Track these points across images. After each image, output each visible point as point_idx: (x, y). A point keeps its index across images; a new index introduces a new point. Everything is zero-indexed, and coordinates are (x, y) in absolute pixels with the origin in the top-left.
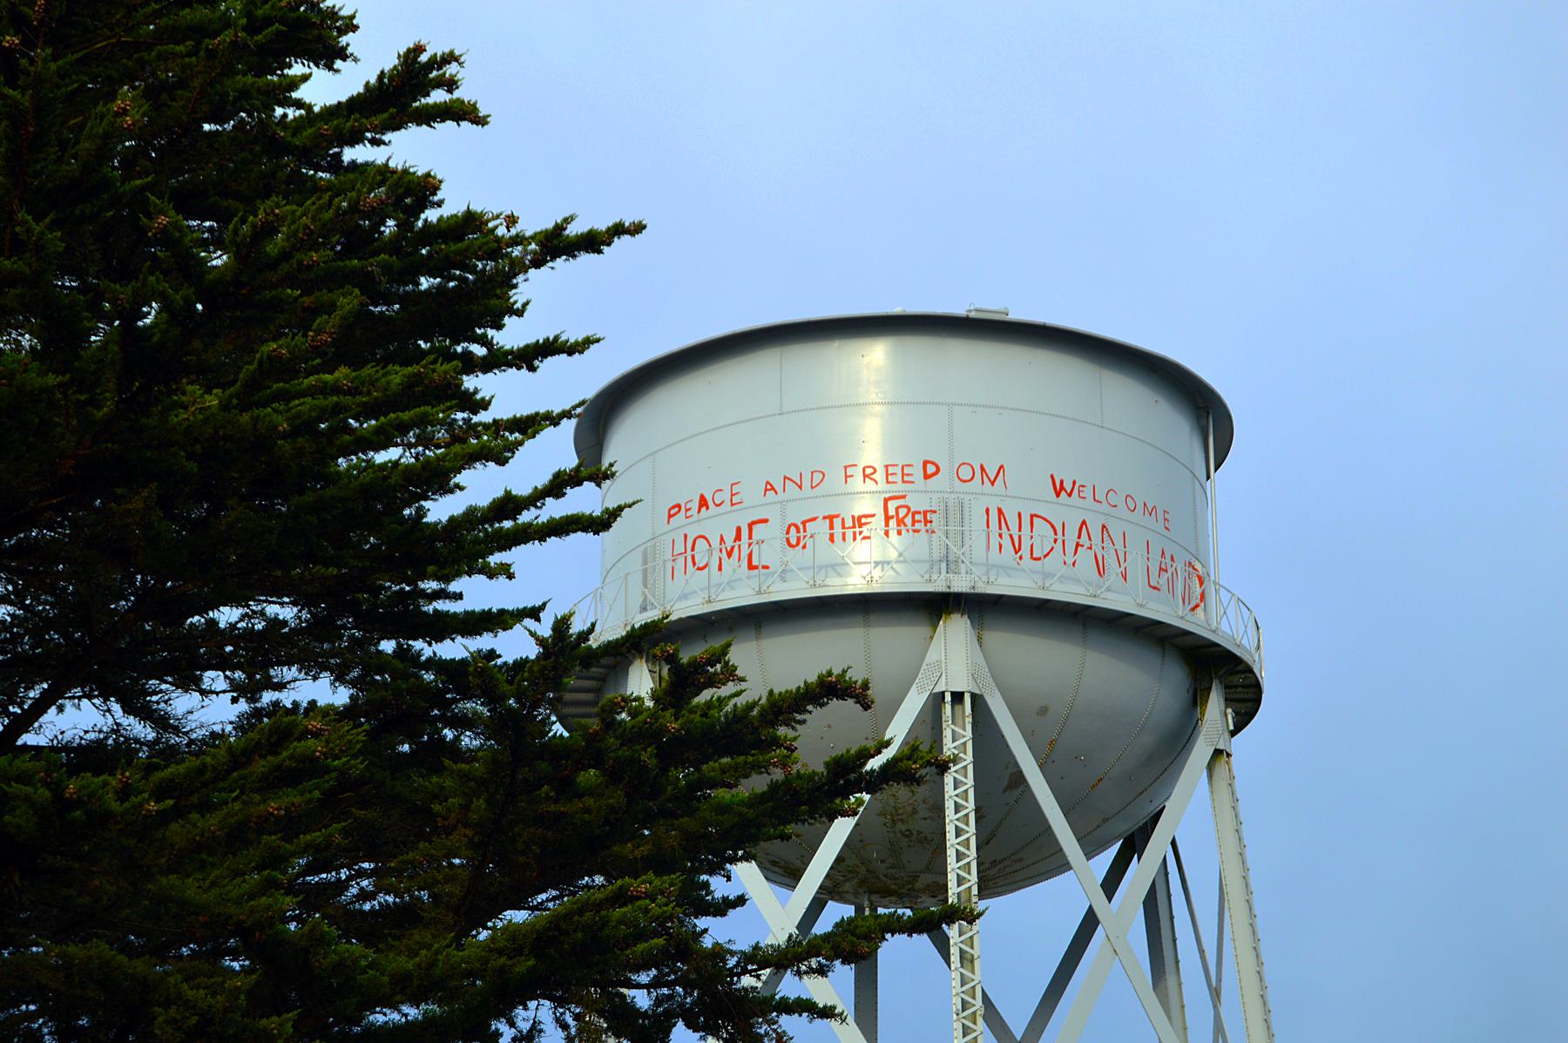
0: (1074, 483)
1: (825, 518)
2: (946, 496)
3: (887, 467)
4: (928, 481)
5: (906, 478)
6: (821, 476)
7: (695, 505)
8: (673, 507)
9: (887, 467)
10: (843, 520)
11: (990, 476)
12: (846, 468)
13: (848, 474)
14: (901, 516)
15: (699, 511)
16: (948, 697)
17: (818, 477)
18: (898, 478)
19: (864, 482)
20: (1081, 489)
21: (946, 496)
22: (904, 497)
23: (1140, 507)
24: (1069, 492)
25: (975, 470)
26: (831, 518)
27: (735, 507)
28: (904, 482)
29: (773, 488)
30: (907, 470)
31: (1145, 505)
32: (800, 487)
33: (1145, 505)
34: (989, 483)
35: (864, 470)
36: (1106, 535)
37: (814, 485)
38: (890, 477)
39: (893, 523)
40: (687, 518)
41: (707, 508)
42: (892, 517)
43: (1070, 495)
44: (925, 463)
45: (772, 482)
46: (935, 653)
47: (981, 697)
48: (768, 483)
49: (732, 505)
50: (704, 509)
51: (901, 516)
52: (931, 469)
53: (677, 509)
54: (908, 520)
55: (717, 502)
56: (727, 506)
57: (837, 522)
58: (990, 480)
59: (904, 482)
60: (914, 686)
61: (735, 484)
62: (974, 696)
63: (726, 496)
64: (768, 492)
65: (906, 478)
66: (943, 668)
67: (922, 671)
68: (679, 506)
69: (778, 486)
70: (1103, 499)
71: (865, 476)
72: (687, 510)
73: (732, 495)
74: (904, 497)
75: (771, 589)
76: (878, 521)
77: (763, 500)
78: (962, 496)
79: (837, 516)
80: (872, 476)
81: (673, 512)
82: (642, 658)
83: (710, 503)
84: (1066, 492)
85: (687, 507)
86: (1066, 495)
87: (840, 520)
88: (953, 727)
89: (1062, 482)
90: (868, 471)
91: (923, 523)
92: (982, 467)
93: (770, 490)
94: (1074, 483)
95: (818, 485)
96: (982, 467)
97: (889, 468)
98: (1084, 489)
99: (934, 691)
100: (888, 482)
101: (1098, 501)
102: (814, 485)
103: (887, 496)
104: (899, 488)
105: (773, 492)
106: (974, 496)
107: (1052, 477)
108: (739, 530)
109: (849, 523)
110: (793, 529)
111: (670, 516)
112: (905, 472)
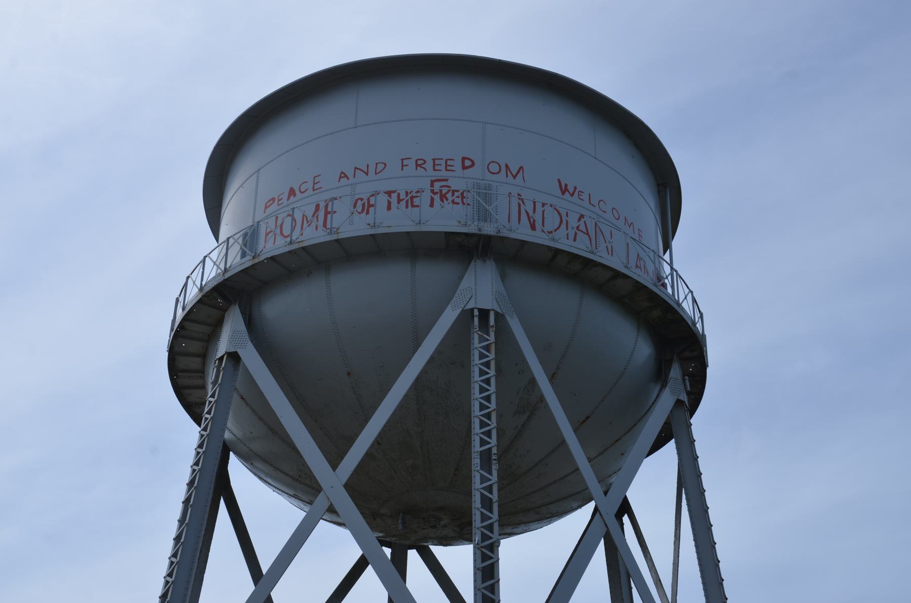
0: (575, 188)
1: (386, 193)
2: (479, 181)
3: (434, 160)
5: (448, 168)
6: (383, 165)
7: (286, 195)
8: (269, 201)
9: (434, 160)
10: (399, 194)
11: (513, 173)
12: (402, 160)
13: (404, 164)
14: (444, 191)
16: (476, 313)
17: (381, 167)
18: (443, 167)
19: (416, 169)
20: (580, 193)
21: (479, 181)
22: (447, 180)
23: (622, 220)
25: (502, 167)
26: (389, 193)
28: (446, 170)
29: (346, 176)
30: (449, 163)
31: (626, 219)
32: (367, 174)
33: (626, 219)
34: (512, 177)
35: (416, 161)
36: (599, 233)
37: (377, 172)
39: (437, 198)
41: (295, 195)
42: (437, 193)
43: (572, 195)
44: (464, 159)
45: (346, 173)
46: (468, 281)
47: (503, 316)
48: (342, 173)
49: (314, 190)
51: (444, 191)
52: (468, 163)
55: (302, 190)
56: (310, 192)
57: (394, 196)
58: (512, 174)
59: (446, 170)
60: (450, 305)
61: (316, 177)
62: (496, 313)
63: (310, 185)
64: (342, 179)
65: (448, 168)
66: (474, 290)
67: (456, 295)
68: (273, 199)
69: (350, 174)
70: (596, 204)
71: (417, 165)
72: (279, 200)
73: (314, 184)
74: (447, 180)
76: (427, 196)
79: (394, 192)
80: (423, 166)
81: (268, 204)
85: (280, 198)
86: (569, 195)
88: (479, 333)
89: (566, 185)
90: (420, 162)
91: (460, 198)
92: (507, 165)
93: (344, 177)
94: (575, 188)
95: (378, 173)
96: (507, 165)
97: (436, 160)
98: (582, 194)
99: (465, 308)
100: (434, 170)
101: (593, 205)
102: (377, 172)
103: (434, 178)
104: (444, 174)
105: (345, 178)
107: (559, 180)
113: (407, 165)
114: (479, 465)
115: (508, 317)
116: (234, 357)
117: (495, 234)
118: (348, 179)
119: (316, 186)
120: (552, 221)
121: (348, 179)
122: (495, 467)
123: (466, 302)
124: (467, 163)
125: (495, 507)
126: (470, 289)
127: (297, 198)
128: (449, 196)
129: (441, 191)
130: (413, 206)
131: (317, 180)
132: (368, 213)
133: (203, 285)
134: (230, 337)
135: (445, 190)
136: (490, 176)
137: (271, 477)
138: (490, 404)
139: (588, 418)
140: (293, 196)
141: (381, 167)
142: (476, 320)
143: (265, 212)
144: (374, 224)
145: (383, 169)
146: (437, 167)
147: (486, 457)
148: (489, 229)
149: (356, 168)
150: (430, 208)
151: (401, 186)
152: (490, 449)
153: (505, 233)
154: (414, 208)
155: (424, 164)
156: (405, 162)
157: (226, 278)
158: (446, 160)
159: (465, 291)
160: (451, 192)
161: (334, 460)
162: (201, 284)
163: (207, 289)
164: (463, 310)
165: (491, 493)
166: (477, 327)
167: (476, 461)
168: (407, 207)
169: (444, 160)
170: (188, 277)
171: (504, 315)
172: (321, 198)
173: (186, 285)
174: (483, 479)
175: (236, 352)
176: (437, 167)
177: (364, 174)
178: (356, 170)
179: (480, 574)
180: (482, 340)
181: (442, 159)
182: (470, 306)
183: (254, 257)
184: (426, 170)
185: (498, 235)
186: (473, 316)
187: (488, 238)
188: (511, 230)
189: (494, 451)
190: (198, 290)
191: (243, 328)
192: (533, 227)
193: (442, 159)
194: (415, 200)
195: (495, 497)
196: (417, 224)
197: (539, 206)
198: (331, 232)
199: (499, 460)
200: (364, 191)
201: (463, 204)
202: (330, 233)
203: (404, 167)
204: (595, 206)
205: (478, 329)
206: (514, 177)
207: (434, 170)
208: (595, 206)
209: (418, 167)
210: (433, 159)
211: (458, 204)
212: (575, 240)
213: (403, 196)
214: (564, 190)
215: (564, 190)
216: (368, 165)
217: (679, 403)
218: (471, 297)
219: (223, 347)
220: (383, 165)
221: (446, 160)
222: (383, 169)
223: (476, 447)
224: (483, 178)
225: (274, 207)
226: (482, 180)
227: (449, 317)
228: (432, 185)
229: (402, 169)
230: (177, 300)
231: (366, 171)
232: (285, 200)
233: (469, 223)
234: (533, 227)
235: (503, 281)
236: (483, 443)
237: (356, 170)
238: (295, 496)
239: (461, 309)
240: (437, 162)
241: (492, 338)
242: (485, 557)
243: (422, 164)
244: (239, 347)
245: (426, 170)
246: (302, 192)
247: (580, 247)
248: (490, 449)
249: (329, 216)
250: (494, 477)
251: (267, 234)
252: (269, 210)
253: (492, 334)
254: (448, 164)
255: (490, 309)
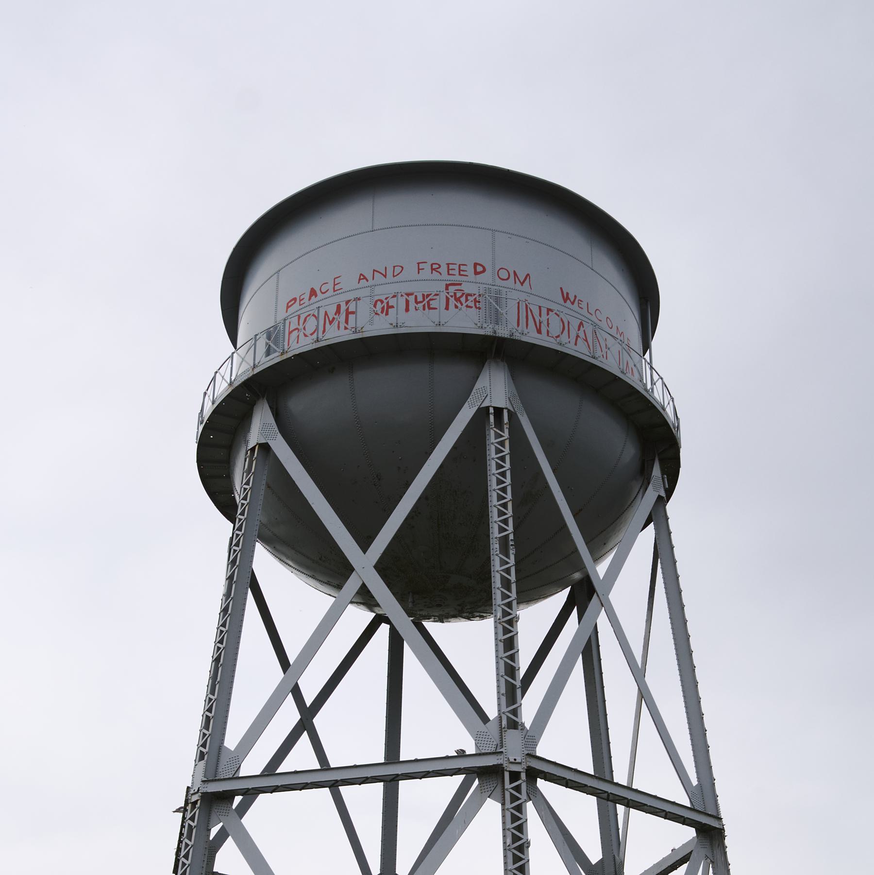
0: (575, 297)
2: (490, 287)
3: (448, 264)
4: (477, 276)
5: (462, 273)
6: (401, 269)
7: (307, 296)
8: (290, 301)
9: (448, 264)
10: (416, 297)
11: (520, 279)
12: (418, 264)
13: (420, 268)
15: (310, 299)
16: (492, 410)
17: (398, 270)
18: (456, 272)
19: (432, 273)
20: (580, 302)
21: (490, 287)
22: (460, 284)
24: (572, 301)
25: (511, 275)
26: (408, 295)
27: (338, 292)
29: (365, 278)
30: (462, 268)
32: (385, 276)
35: (432, 265)
37: (395, 274)
38: (450, 271)
39: (452, 300)
40: (300, 305)
41: (316, 296)
43: (573, 303)
44: (476, 265)
46: (483, 382)
48: (361, 274)
49: (334, 291)
50: (313, 297)
52: (479, 269)
53: (293, 301)
54: (463, 299)
55: (323, 291)
56: (331, 292)
58: (520, 281)
59: (460, 275)
60: (467, 403)
61: (336, 278)
62: (509, 411)
63: (330, 286)
64: (361, 281)
65: (462, 273)
66: (489, 389)
67: (472, 394)
68: (295, 299)
69: (370, 277)
71: (432, 269)
72: (300, 300)
73: (335, 285)
75: (364, 330)
77: (360, 285)
78: (501, 288)
79: (412, 294)
80: (437, 270)
81: (290, 304)
82: (263, 397)
83: (318, 292)
84: (571, 302)
85: (302, 298)
86: (570, 303)
87: (413, 297)
88: (495, 429)
89: (567, 294)
90: (435, 266)
93: (362, 279)
94: (575, 297)
95: (396, 276)
97: (450, 265)
99: (481, 406)
100: (449, 274)
102: (395, 275)
103: (448, 282)
104: (458, 278)
105: (365, 280)
106: (509, 290)
107: (561, 288)
108: (339, 307)
109: (420, 299)
110: (379, 303)
111: (288, 307)
112: (461, 269)
113: (423, 269)
114: (498, 549)
115: (519, 415)
116: (265, 448)
117: (509, 337)
118: (367, 281)
119: (337, 287)
120: (555, 327)
121: (367, 281)
122: (512, 552)
123: (482, 400)
124: (479, 269)
125: (514, 587)
126: (485, 388)
127: (318, 298)
128: (463, 299)
129: (455, 294)
130: (430, 308)
131: (337, 281)
132: (387, 314)
133: (233, 380)
134: (261, 429)
135: (459, 294)
136: (498, 282)
137: (292, 560)
138: (506, 494)
139: (581, 510)
140: (314, 296)
141: (398, 270)
142: (492, 417)
143: (287, 311)
144: (397, 324)
145: (400, 273)
146: (451, 272)
147: (504, 541)
148: (503, 332)
149: (374, 270)
150: (446, 310)
151: (420, 289)
152: (507, 536)
153: (517, 336)
154: (431, 310)
155: (438, 268)
156: (421, 266)
157: (255, 373)
158: (460, 265)
159: (481, 389)
160: (465, 295)
161: (365, 544)
162: (231, 379)
163: (236, 384)
164: (479, 408)
165: (509, 574)
166: (493, 424)
167: (495, 546)
168: (424, 309)
169: (458, 266)
170: (216, 372)
171: (516, 414)
172: (341, 299)
173: (214, 379)
174: (503, 563)
175: (267, 443)
176: (451, 272)
177: (382, 276)
178: (375, 272)
179: (501, 645)
180: (498, 436)
181: (456, 264)
182: (485, 405)
183: (282, 354)
184: (441, 274)
185: (512, 338)
186: (488, 414)
187: (503, 340)
188: (523, 334)
189: (511, 537)
190: (227, 385)
191: (271, 420)
192: (539, 331)
193: (456, 264)
194: (431, 302)
195: (513, 578)
196: (437, 325)
197: (544, 311)
198: (356, 331)
199: (516, 546)
200: (382, 292)
201: (476, 307)
202: (355, 332)
203: (420, 271)
204: (592, 314)
205: (493, 426)
206: (522, 284)
207: (449, 274)
208: (592, 314)
209: (433, 271)
210: (447, 264)
211: (471, 307)
212: (576, 344)
213: (420, 299)
214: (566, 298)
215: (566, 298)
216: (386, 268)
217: (660, 497)
218: (487, 395)
219: (254, 437)
220: (400, 268)
221: (460, 265)
222: (400, 273)
223: (495, 533)
224: (494, 284)
225: (296, 306)
226: (493, 285)
227: (466, 415)
228: (447, 289)
229: (419, 273)
230: (205, 394)
231: (384, 274)
232: (306, 300)
233: (485, 325)
234: (539, 331)
235: (513, 380)
236: (502, 530)
237: (375, 272)
238: (313, 577)
239: (477, 407)
240: (451, 267)
241: (506, 434)
242: (506, 631)
243: (438, 268)
244: (270, 438)
245: (441, 274)
246: (323, 293)
247: (579, 350)
248: (508, 534)
249: (350, 316)
250: (512, 561)
251: (290, 333)
252: (291, 310)
253: (506, 431)
254: (461, 269)
255: (504, 407)
